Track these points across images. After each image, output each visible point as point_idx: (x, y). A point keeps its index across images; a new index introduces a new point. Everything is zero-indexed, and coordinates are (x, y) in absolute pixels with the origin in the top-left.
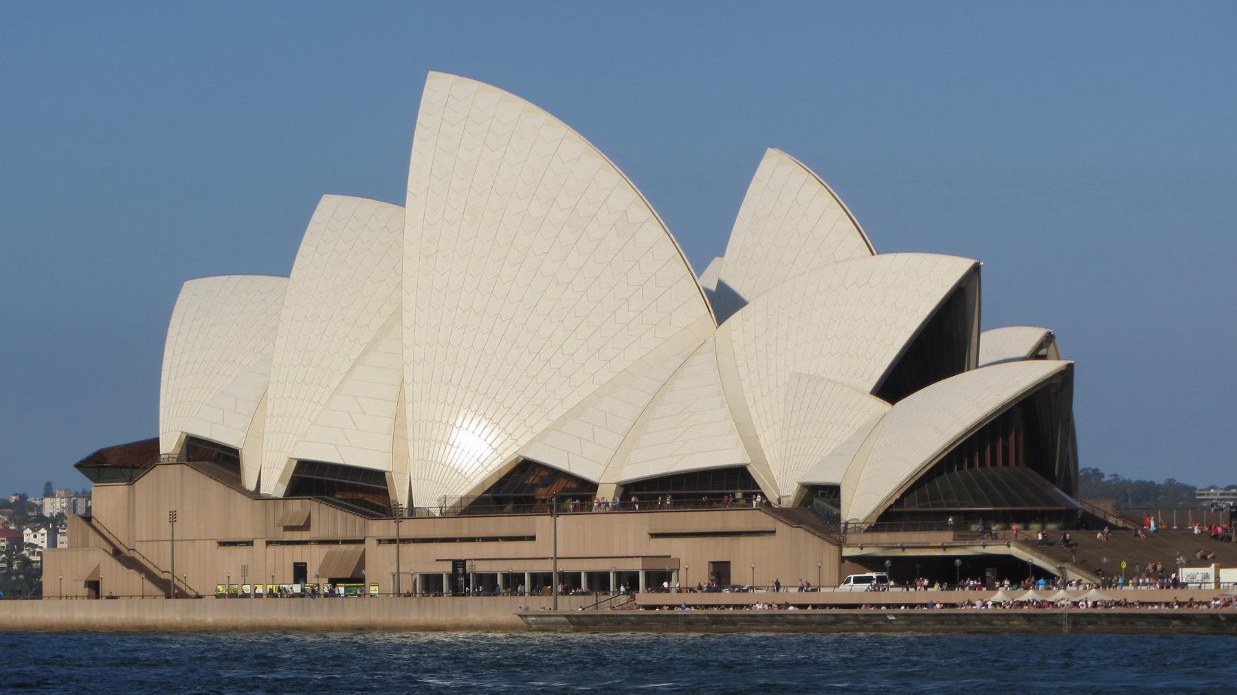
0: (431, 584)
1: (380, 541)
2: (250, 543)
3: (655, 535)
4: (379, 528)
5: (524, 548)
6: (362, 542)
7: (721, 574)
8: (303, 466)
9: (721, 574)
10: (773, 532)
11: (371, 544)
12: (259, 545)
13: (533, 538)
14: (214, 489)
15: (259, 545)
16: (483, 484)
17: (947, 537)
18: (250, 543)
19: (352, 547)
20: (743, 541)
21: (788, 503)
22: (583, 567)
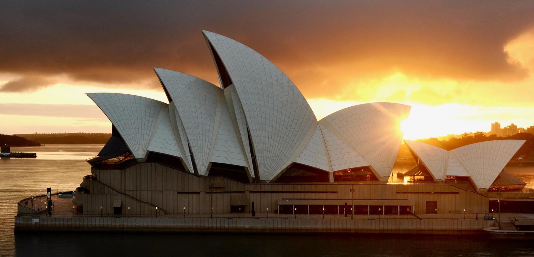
1: (251, 192)
2: (199, 193)
3: (397, 193)
4: (250, 187)
5: (332, 196)
6: (244, 192)
10: (458, 193)
11: (247, 193)
13: (336, 192)
14: (175, 173)
16: (282, 172)
18: (199, 193)
19: (240, 194)
20: (443, 195)
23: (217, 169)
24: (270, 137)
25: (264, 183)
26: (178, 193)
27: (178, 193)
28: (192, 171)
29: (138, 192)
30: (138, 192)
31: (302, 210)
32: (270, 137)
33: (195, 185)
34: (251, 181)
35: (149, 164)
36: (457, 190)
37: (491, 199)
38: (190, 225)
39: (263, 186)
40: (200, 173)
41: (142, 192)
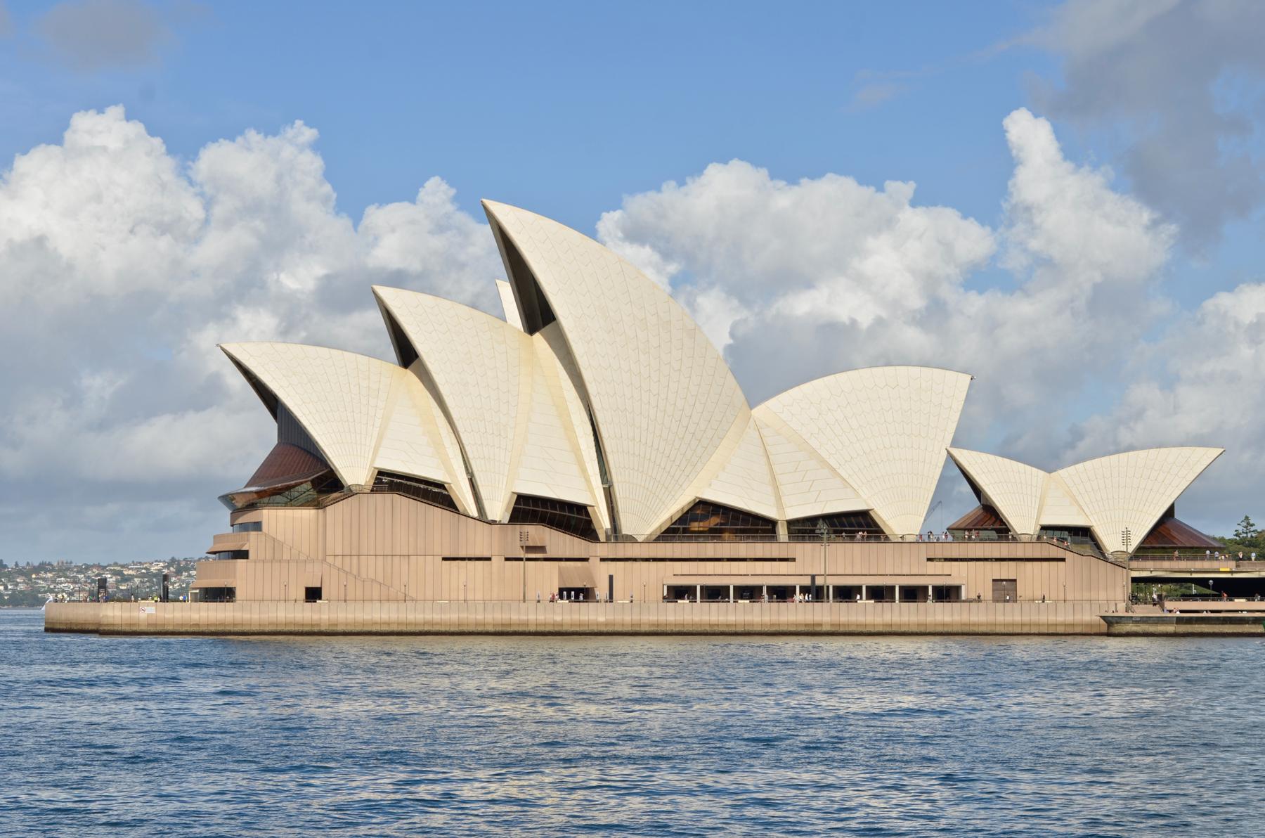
0: (678, 593)
1: (602, 560)
2: (489, 559)
3: (929, 560)
5: (783, 567)
7: (1005, 590)
8: (522, 499)
9: (1005, 590)
10: (1063, 560)
11: (594, 562)
12: (497, 561)
13: (794, 560)
14: (437, 514)
15: (497, 561)
17: (1231, 565)
18: (489, 559)
19: (579, 564)
20: (1029, 564)
21: (1024, 538)
22: (898, 582)
23: (529, 509)
24: (643, 441)
25: (630, 539)
26: (444, 559)
27: (444, 559)
28: (475, 513)
29: (355, 559)
30: (355, 559)
31: (715, 593)
32: (643, 441)
33: (479, 540)
34: (602, 537)
35: (379, 497)
36: (1060, 553)
37: (1136, 574)
38: (480, 617)
39: (629, 545)
40: (490, 518)
41: (362, 558)
